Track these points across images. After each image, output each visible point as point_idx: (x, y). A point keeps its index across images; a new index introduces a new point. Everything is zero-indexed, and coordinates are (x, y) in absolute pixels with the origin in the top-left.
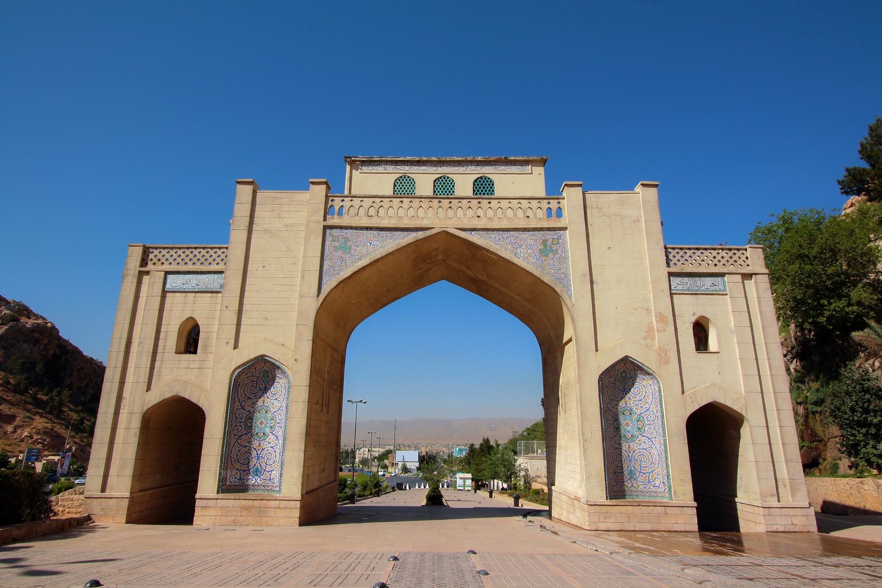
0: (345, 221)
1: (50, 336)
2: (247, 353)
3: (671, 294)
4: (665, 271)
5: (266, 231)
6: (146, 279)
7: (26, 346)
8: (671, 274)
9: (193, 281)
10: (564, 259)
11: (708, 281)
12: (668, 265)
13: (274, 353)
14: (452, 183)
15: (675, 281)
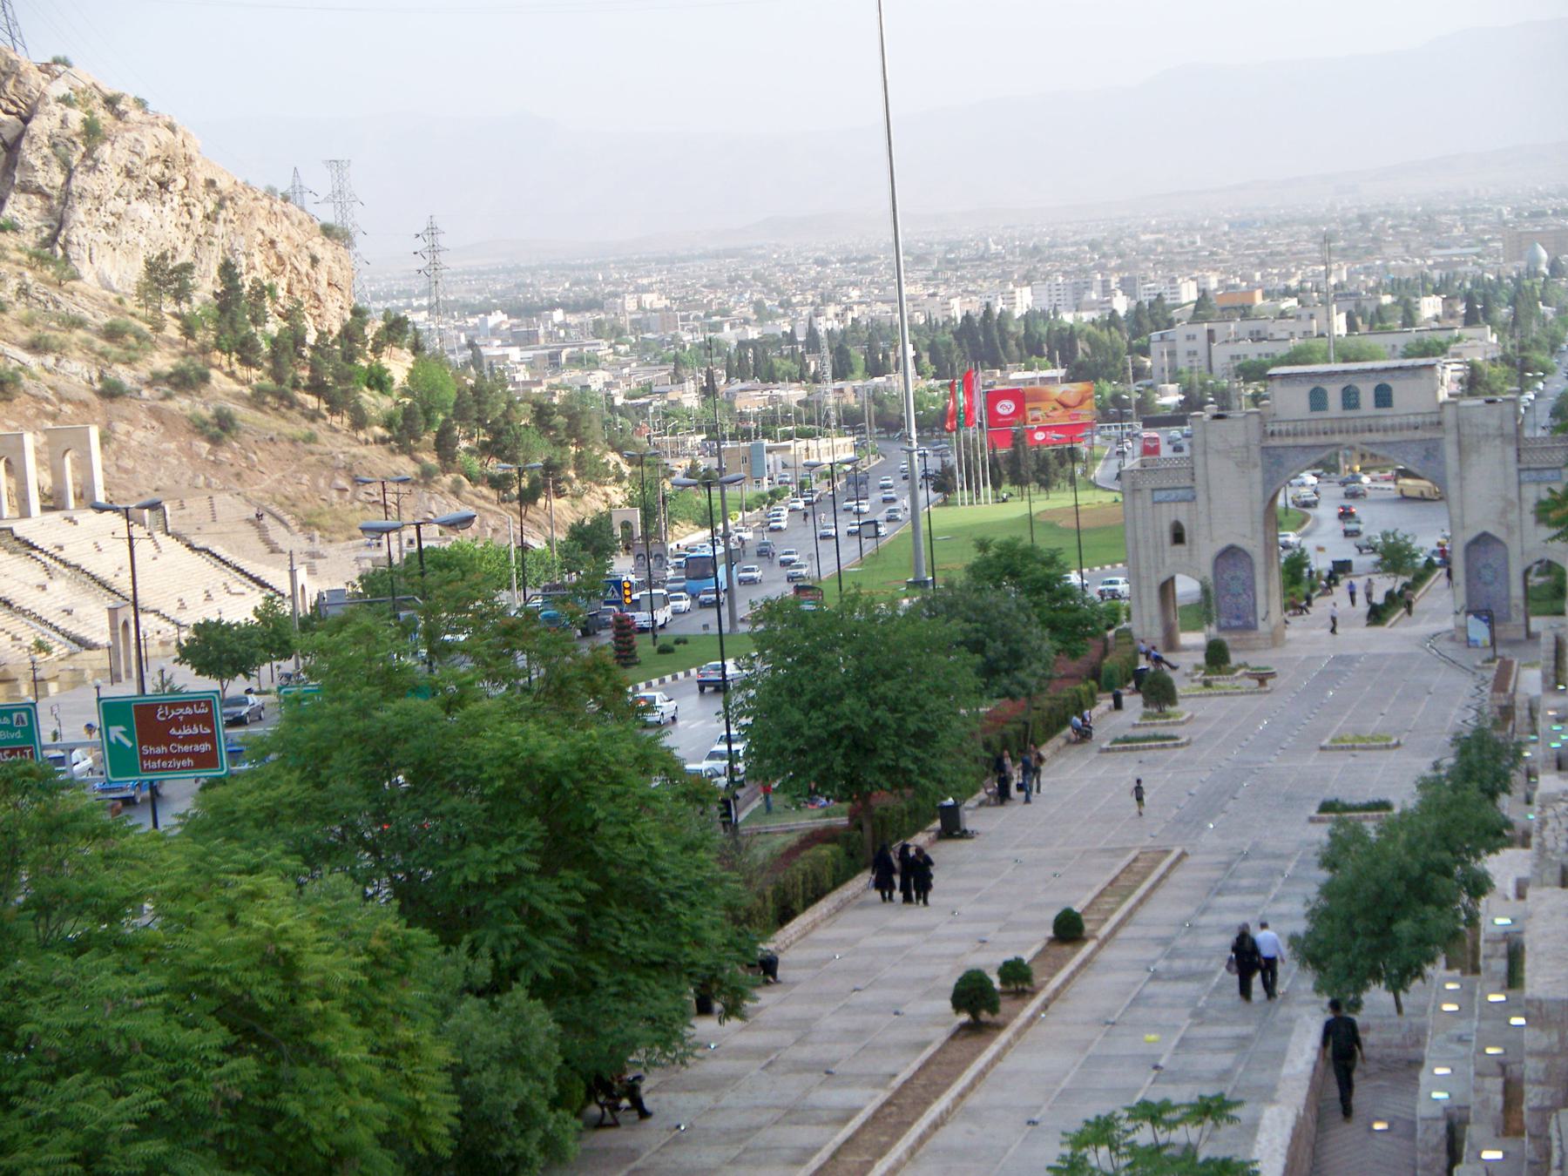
0: (1276, 442)
1: (189, 160)
2: (1222, 544)
3: (1520, 483)
4: (1513, 470)
5: (1218, 451)
6: (1138, 495)
7: (144, 209)
8: (1520, 470)
9: (1173, 494)
10: (1442, 463)
11: (1548, 474)
12: (1519, 461)
13: (1240, 543)
14: (1357, 393)
15: (1524, 476)
